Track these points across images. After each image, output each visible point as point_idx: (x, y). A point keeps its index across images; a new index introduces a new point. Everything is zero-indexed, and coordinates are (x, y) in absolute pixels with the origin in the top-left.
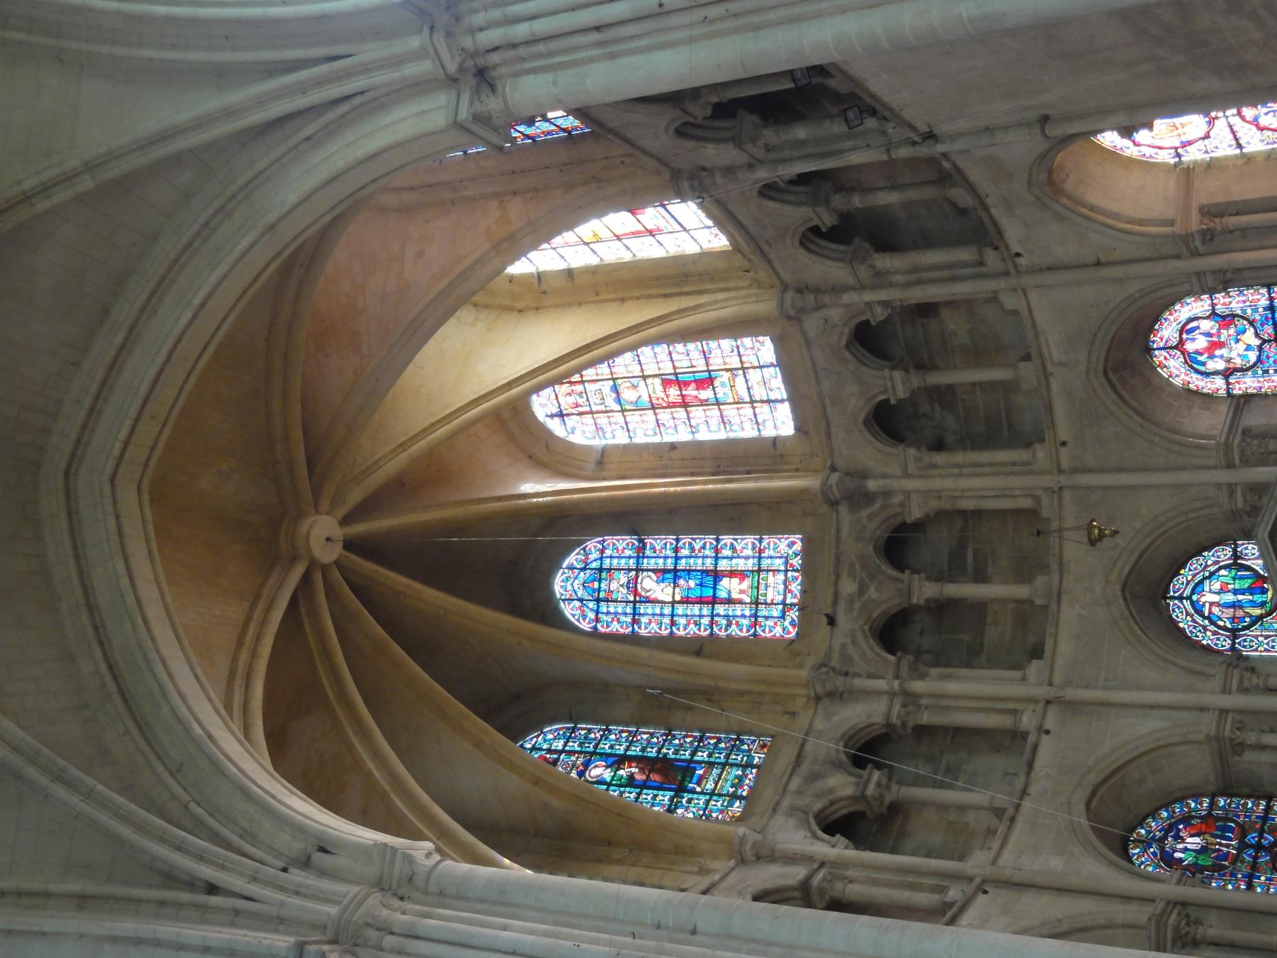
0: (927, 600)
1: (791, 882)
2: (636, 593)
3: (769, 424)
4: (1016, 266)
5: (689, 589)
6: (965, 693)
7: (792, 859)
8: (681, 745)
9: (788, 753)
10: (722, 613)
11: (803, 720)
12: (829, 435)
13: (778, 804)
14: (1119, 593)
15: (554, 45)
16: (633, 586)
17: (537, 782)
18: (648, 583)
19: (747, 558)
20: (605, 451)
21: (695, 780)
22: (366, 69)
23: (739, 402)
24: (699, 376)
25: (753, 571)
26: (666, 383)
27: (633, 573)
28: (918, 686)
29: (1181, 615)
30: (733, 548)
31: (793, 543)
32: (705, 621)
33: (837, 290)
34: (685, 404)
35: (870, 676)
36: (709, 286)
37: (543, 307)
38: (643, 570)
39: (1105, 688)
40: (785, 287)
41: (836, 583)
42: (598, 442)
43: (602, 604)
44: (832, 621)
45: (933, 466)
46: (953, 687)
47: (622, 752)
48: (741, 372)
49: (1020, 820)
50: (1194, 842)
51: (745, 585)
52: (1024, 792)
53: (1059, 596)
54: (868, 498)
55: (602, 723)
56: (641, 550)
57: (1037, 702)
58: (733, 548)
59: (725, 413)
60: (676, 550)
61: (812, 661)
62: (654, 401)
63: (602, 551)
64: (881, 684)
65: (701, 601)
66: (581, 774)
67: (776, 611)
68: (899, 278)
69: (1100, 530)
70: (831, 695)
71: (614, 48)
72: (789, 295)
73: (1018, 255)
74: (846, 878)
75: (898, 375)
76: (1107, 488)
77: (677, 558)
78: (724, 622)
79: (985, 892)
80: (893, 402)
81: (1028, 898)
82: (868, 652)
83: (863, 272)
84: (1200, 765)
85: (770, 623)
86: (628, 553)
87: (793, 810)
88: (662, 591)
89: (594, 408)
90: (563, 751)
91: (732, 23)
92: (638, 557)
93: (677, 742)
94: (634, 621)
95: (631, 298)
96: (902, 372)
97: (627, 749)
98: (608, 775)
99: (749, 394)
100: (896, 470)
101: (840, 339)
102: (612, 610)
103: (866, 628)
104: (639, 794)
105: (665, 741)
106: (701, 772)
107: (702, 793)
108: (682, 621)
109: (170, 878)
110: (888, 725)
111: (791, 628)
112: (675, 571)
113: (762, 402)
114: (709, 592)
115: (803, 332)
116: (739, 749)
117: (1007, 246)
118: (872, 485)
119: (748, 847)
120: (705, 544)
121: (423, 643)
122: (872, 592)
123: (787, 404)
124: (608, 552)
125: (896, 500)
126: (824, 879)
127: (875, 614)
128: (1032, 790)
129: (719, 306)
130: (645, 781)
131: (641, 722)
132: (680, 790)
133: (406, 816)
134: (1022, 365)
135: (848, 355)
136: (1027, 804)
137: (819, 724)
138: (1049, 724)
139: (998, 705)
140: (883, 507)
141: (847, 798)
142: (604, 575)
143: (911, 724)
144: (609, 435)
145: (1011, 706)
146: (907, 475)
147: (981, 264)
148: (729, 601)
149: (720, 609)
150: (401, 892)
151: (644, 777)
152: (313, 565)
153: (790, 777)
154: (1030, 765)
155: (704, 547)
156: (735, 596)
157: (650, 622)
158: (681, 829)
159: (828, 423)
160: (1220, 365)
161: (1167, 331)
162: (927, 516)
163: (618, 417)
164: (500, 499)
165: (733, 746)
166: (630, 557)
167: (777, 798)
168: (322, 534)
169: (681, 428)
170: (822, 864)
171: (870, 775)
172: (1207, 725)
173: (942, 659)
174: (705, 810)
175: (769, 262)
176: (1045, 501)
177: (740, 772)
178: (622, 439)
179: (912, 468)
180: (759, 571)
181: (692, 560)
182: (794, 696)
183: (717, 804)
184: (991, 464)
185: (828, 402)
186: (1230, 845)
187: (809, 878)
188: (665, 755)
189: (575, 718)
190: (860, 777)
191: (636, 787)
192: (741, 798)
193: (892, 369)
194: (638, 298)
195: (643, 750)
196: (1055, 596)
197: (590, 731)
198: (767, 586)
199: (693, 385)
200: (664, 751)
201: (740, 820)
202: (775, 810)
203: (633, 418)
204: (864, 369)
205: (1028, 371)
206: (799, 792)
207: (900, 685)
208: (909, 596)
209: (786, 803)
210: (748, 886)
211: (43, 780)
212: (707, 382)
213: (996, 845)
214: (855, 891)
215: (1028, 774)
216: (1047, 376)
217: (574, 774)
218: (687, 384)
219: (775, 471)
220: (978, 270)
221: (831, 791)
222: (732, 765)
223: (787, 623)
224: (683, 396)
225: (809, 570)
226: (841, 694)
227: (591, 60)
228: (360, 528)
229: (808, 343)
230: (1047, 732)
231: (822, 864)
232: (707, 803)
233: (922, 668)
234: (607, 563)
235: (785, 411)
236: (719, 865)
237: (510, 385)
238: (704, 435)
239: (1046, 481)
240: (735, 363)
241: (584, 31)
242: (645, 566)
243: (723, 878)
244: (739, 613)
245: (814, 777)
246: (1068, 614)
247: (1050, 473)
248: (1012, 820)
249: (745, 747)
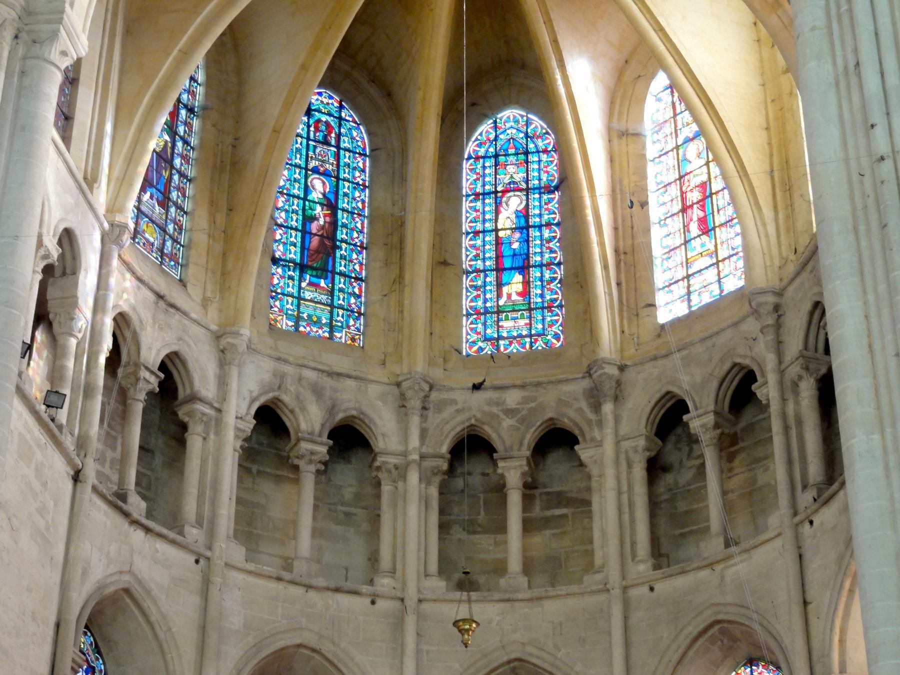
0: (502, 476)
1: (197, 385)
2: (504, 192)
3: (669, 298)
4: (802, 522)
5: (510, 244)
6: (411, 518)
7: (223, 381)
8: (351, 261)
9: (341, 364)
10: (488, 279)
11: (378, 373)
12: (655, 358)
13: (286, 361)
14: (513, 656)
15: (846, 20)
17: (276, 131)
18: (515, 202)
19: (542, 296)
20: (638, 135)
21: (314, 280)
23: (688, 263)
24: (710, 218)
25: (529, 303)
26: (703, 186)
27: (524, 186)
28: (413, 477)
30: (553, 279)
31: (558, 339)
32: (479, 264)
33: (779, 346)
34: (684, 209)
35: (423, 434)
36: (781, 216)
37: (760, 47)
38: (527, 195)
39: (418, 652)
40: (780, 294)
41: (514, 386)
42: (648, 126)
43: (493, 160)
44: (477, 387)
45: (630, 466)
46: (413, 510)
47: (340, 205)
48: (714, 261)
49: (280, 586)
51: (515, 297)
52: (309, 587)
53: (508, 600)
54: (597, 407)
55: (370, 182)
56: (549, 189)
57: (403, 590)
58: (553, 279)
59: (677, 251)
60: (548, 225)
61: (437, 374)
62: (686, 177)
63: (545, 151)
64: (414, 441)
65: (499, 257)
66: (315, 170)
67: (491, 332)
68: (791, 407)
69: (467, 631)
70: (402, 396)
71: (842, 85)
72: (771, 299)
73: (811, 522)
74: (208, 434)
75: (710, 419)
76: (609, 633)
77: (540, 227)
78: (480, 283)
79: (197, 562)
80: (685, 418)
81: (194, 600)
83: (794, 370)
85: (480, 328)
86: (544, 177)
88: (507, 219)
89: (679, 118)
90: (338, 147)
91: (859, 205)
92: (539, 188)
93: (354, 256)
94: (477, 195)
95: (770, 138)
96: (712, 423)
97: (343, 210)
98: (315, 195)
99: (695, 273)
100: (624, 430)
101: (741, 356)
102: (487, 171)
103: (473, 421)
104: (296, 229)
105: (355, 245)
106: (322, 283)
107: (300, 288)
108: (479, 242)
110: (376, 455)
111: (475, 348)
112: (528, 227)
113: (689, 287)
114: (507, 263)
115: (744, 318)
116: (349, 316)
117: (816, 511)
118: (608, 408)
119: (230, 340)
120: (555, 252)
122: (507, 422)
123: (687, 311)
124: (544, 157)
125: (597, 434)
126: (204, 414)
127: (486, 428)
128: (312, 594)
129: (761, 228)
130: (311, 233)
131: (372, 219)
132: (302, 268)
133: (198, 15)
134: (721, 540)
135: (727, 366)
136: (298, 591)
137: (373, 389)
138: (380, 603)
139: (399, 554)
140: (589, 422)
141: (298, 425)
142: (522, 157)
143: (380, 475)
144: (656, 137)
145: (399, 566)
146: (617, 443)
147: (805, 487)
148: (499, 285)
149: (491, 278)
150: (24, 36)
151: (314, 231)
153: (314, 369)
154: (337, 590)
155: (552, 251)
156: (505, 290)
157: (476, 211)
159: (666, 356)
162: (582, 465)
163: (671, 144)
164: (555, 41)
165: (352, 311)
166: (540, 180)
167: (291, 359)
169: (664, 209)
170: (219, 411)
171: (321, 444)
174: (283, 294)
175: (798, 274)
176: (598, 577)
177: (324, 321)
178: (651, 151)
179: (626, 444)
180: (530, 310)
181: (538, 242)
182: (400, 360)
183: (289, 304)
184: (633, 521)
185: (685, 352)
187: (201, 400)
188: (340, 248)
190: (320, 435)
191: (304, 225)
192: (297, 326)
193: (716, 413)
194: (769, 144)
195: (344, 226)
196: (507, 596)
197: (363, 171)
198: (514, 319)
199: (701, 214)
200: (344, 246)
201: (272, 327)
202: (278, 359)
203: (671, 160)
204: (715, 384)
206: (300, 379)
207: (414, 461)
208: (503, 459)
209: (288, 369)
210: (189, 346)
212: (706, 228)
213: (251, 567)
214: (195, 443)
215: (327, 589)
216: (710, 565)
217: (312, 164)
218: (703, 206)
219: (621, 311)
221: (303, 409)
222: (331, 313)
223: (480, 344)
224: (691, 206)
225: (531, 358)
226: (404, 406)
227: (834, 63)
229: (735, 324)
230: (373, 603)
231: (219, 411)
232: (292, 296)
233: (437, 480)
234: (533, 158)
235: (681, 310)
236: (212, 319)
237: (660, 30)
238: (656, 234)
239: (614, 575)
240: (723, 253)
241: (856, 51)
242: (531, 196)
243: (195, 321)
244: (488, 296)
245: (318, 392)
247: (624, 578)
248: (279, 579)
249: (352, 322)
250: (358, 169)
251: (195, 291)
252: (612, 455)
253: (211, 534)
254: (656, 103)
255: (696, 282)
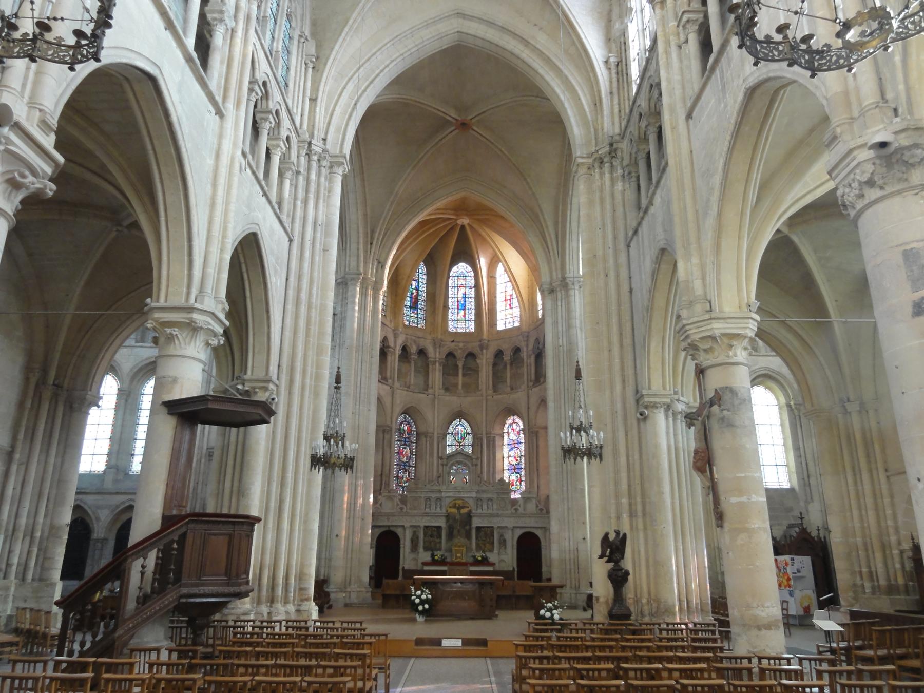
6: (436, 376)
7: (395, 342)
9: (420, 334)
16: (462, 286)
22: (555, 262)
28: (437, 365)
29: (457, 422)
33: (527, 346)
50: (406, 428)
54: (482, 350)
56: (470, 288)
82: (445, 351)
83: (531, 352)
84: (423, 429)
87: (407, 339)
88: (460, 295)
99: (507, 317)
109: (373, 232)
121: (443, 240)
132: (411, 307)
137: (428, 341)
152: (456, 220)
158: (401, 310)
160: (510, 430)
161: (518, 420)
168: (465, 221)
172: (431, 430)
173: (445, 366)
186: (405, 435)
189: (427, 275)
201: (405, 326)
205: (509, 389)
211: (391, 199)
212: (511, 308)
214: (389, 358)
220: (529, 380)
228: (467, 228)
236: (392, 326)
245: (415, 342)
246: (455, 398)
250: (424, 279)
251: (388, 318)
252: (485, 362)
253: (393, 381)
254: (500, 269)
255: (507, 321)
